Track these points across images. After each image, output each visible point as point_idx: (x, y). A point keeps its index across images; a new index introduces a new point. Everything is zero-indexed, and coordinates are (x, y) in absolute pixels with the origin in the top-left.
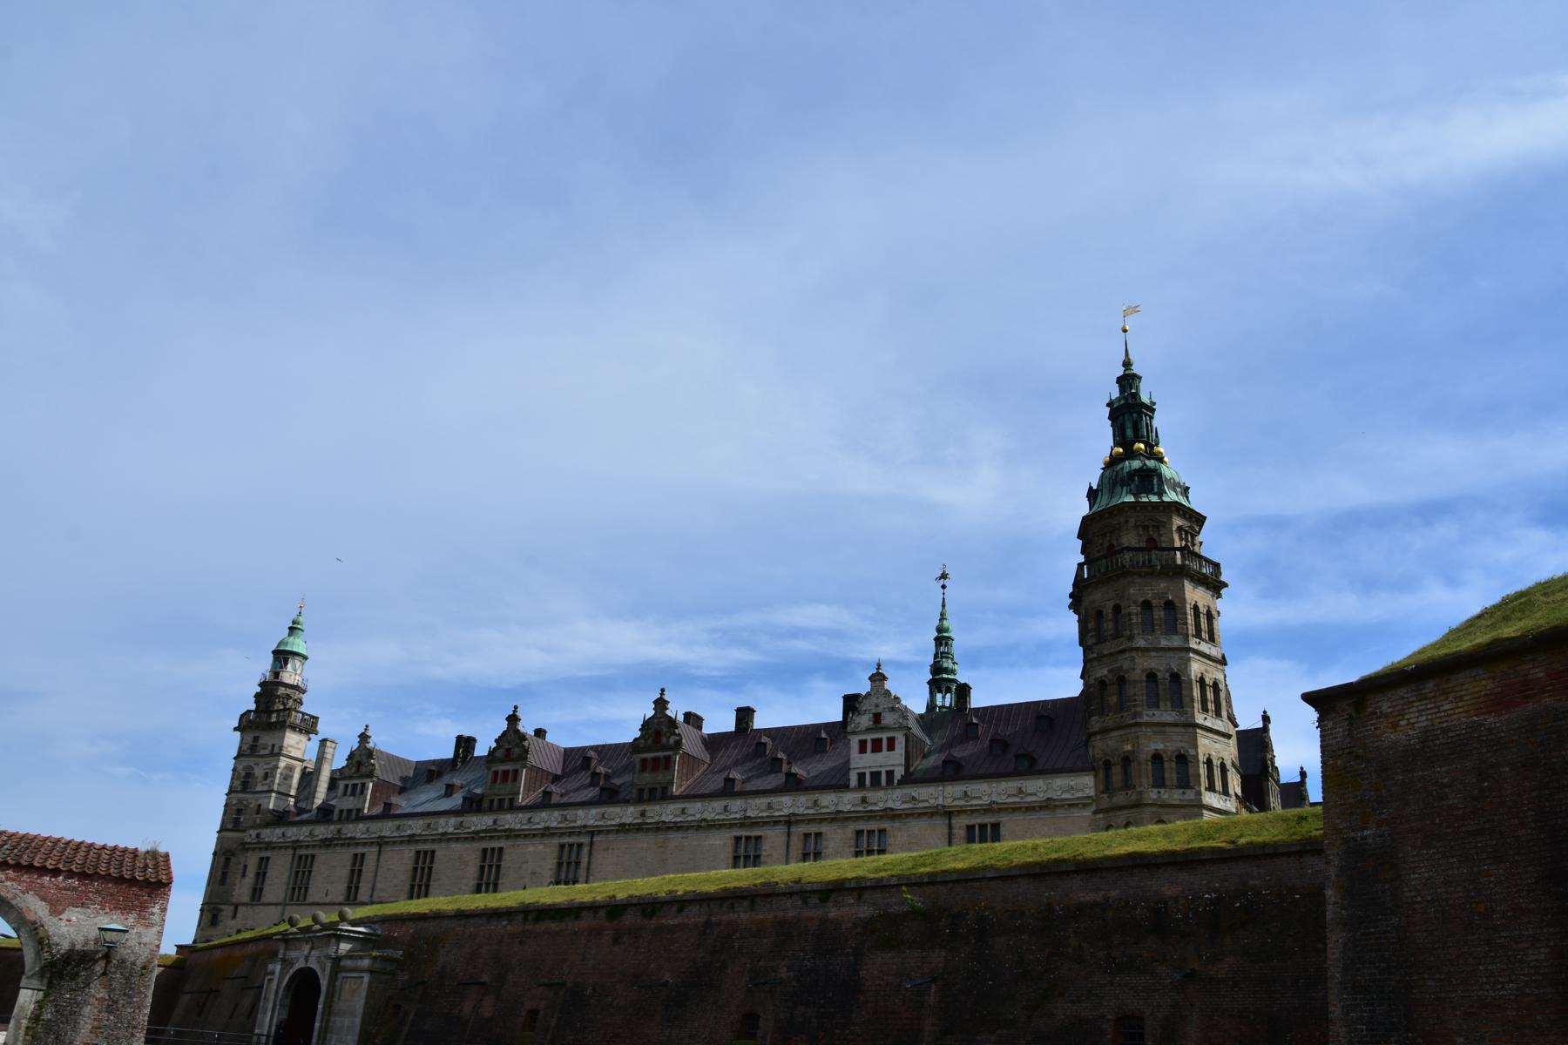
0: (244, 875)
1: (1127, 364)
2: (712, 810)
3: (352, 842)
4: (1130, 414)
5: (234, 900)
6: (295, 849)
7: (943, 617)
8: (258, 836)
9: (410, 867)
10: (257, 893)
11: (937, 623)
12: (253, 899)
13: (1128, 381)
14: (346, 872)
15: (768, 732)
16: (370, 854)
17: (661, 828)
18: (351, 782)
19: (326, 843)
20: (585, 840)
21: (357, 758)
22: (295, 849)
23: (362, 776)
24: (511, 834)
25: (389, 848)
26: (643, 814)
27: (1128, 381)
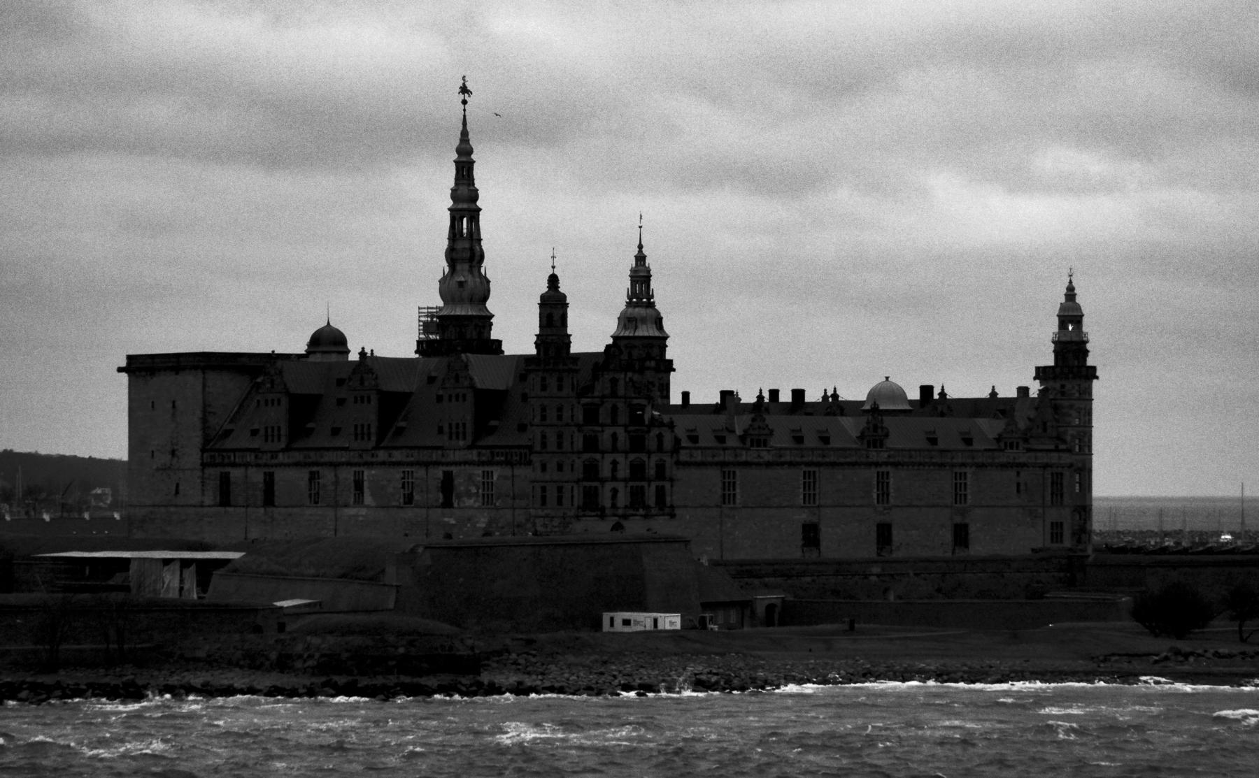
1: (640, 247)
13: (641, 258)
27: (641, 258)
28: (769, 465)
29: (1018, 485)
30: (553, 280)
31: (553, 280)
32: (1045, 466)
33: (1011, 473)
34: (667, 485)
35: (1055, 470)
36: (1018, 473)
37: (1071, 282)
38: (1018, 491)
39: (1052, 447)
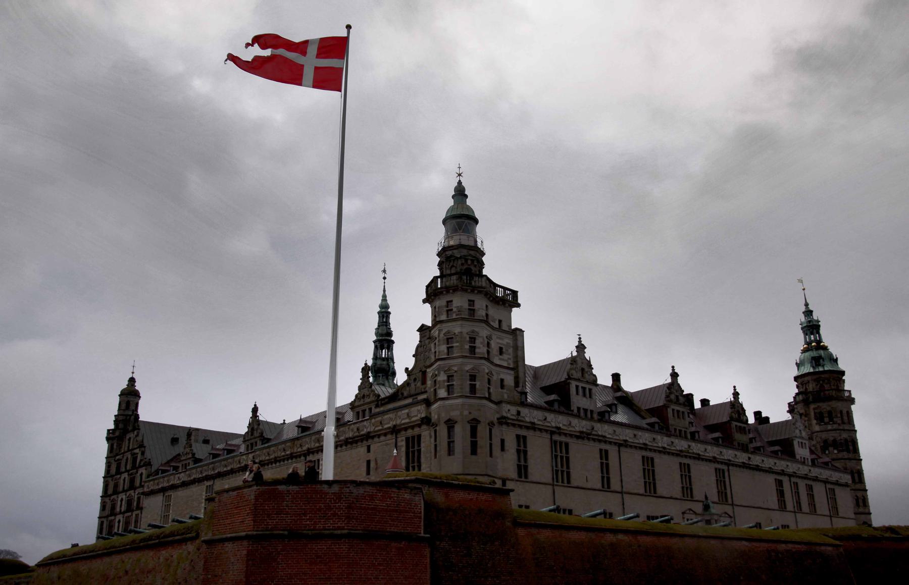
0: (503, 449)
1: (807, 305)
2: (769, 463)
3: (602, 439)
4: (811, 327)
5: (500, 474)
6: (552, 433)
7: (384, 298)
8: (519, 413)
9: (641, 467)
10: (523, 471)
11: (380, 302)
12: (520, 475)
13: (808, 313)
14: (597, 463)
15: (774, 424)
16: (613, 451)
17: (757, 468)
18: (581, 385)
19: (582, 436)
20: (725, 468)
21: (579, 365)
22: (552, 433)
23: (587, 382)
24: (698, 457)
25: (629, 450)
26: (749, 458)
27: (808, 313)
28: (185, 484)
29: (368, 462)
30: (132, 381)
31: (132, 381)
32: (395, 431)
33: (361, 450)
34: (138, 512)
35: (410, 433)
36: (369, 451)
37: (460, 183)
38: (368, 473)
39: (409, 401)
